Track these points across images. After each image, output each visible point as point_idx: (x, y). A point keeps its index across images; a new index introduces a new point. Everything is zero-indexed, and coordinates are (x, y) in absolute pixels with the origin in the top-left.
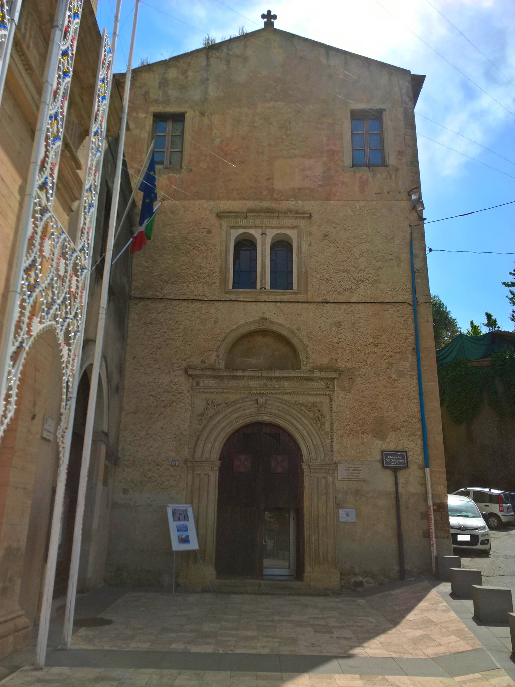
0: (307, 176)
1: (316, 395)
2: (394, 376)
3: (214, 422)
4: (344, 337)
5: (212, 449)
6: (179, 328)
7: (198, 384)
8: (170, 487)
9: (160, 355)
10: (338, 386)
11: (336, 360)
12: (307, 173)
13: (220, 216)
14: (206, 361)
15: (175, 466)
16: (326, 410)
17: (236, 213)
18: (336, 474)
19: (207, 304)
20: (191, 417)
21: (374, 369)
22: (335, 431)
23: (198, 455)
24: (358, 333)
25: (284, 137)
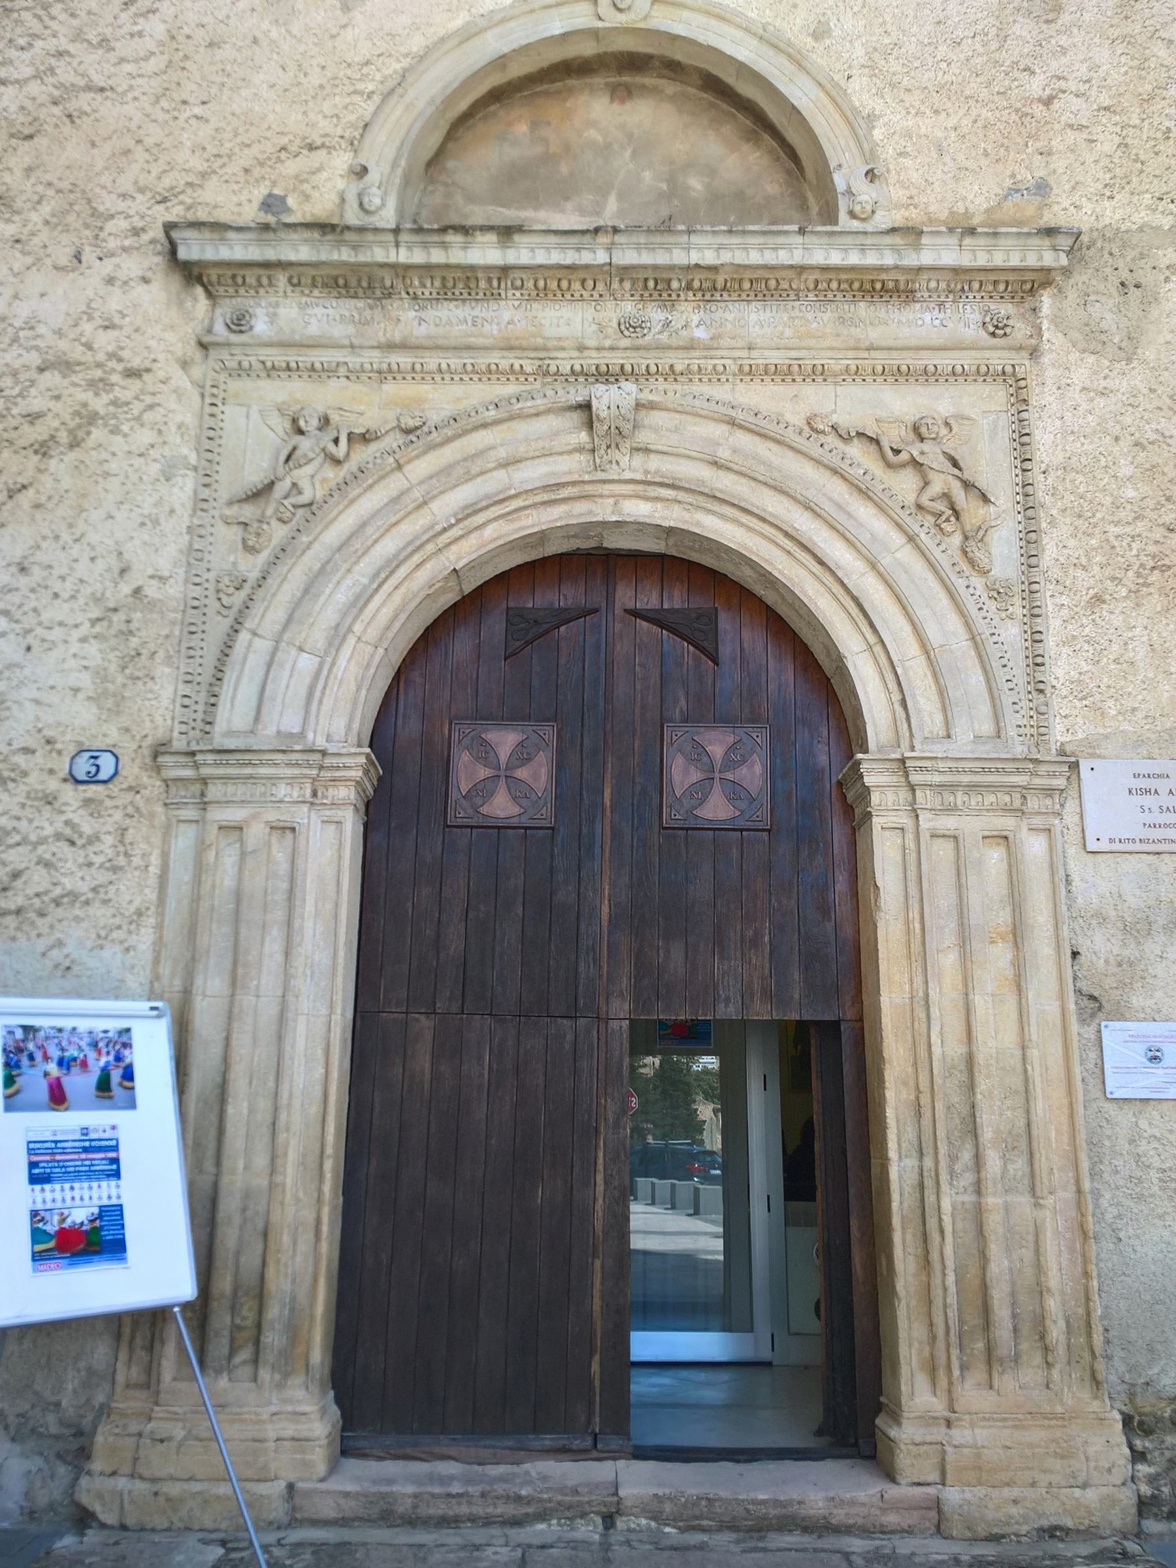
1: (928, 375)
3: (333, 535)
4: (1084, 68)
5: (320, 684)
6: (140, 34)
7: (239, 324)
8: (57, 902)
9: (29, 170)
10: (1056, 321)
11: (1042, 188)
14: (291, 201)
15: (92, 779)
16: (992, 465)
18: (1071, 818)
20: (200, 504)
22: (1055, 573)
23: (233, 716)
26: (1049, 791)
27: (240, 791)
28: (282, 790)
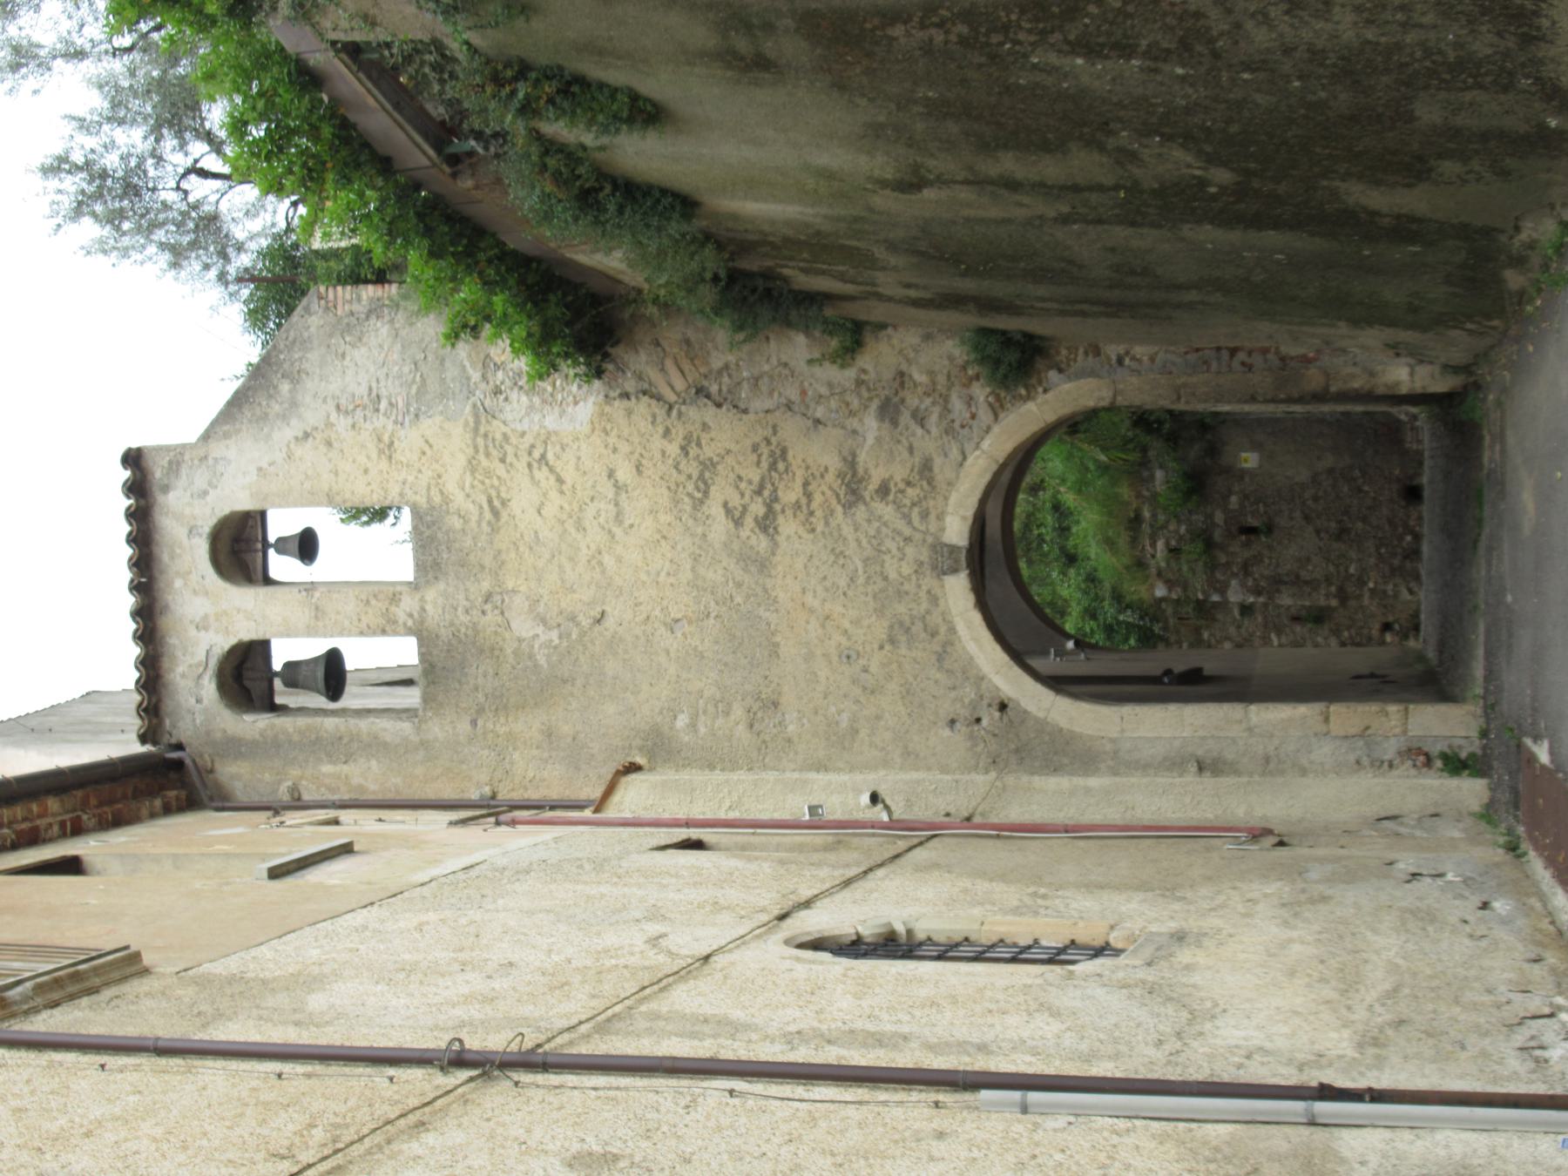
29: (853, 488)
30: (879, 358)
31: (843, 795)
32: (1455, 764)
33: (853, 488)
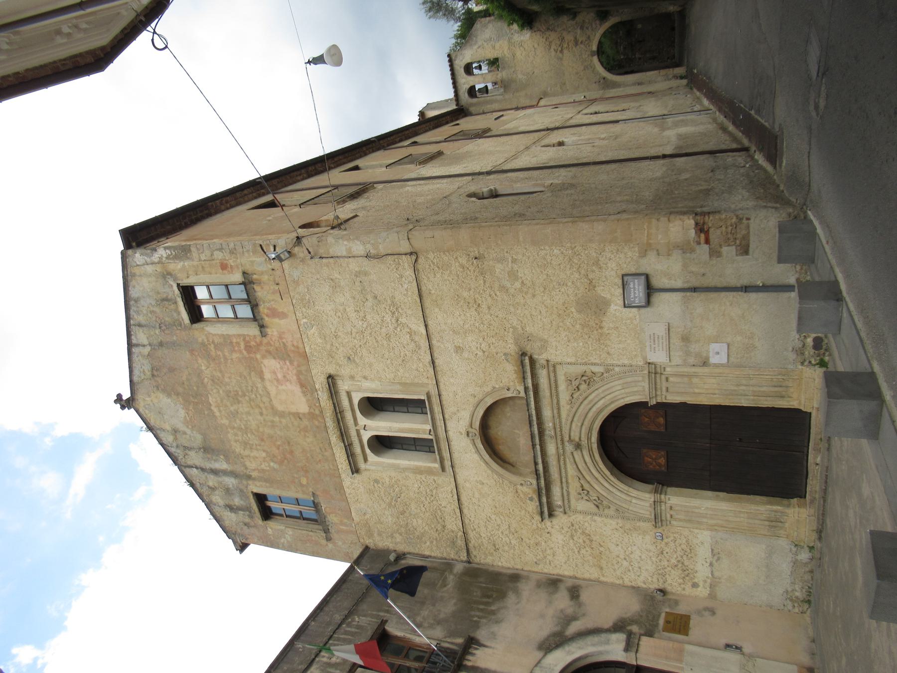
0: (284, 377)
1: (556, 381)
2: (518, 285)
5: (639, 498)
10: (539, 355)
11: (505, 354)
12: (280, 376)
13: (355, 470)
17: (348, 457)
19: (461, 490)
20: (601, 516)
21: (512, 309)
24: (466, 326)
25: (247, 398)
26: (655, 368)
27: (663, 515)
28: (663, 508)
29: (576, 43)
30: (580, 18)
31: (580, 97)
32: (682, 78)
33: (576, 43)
